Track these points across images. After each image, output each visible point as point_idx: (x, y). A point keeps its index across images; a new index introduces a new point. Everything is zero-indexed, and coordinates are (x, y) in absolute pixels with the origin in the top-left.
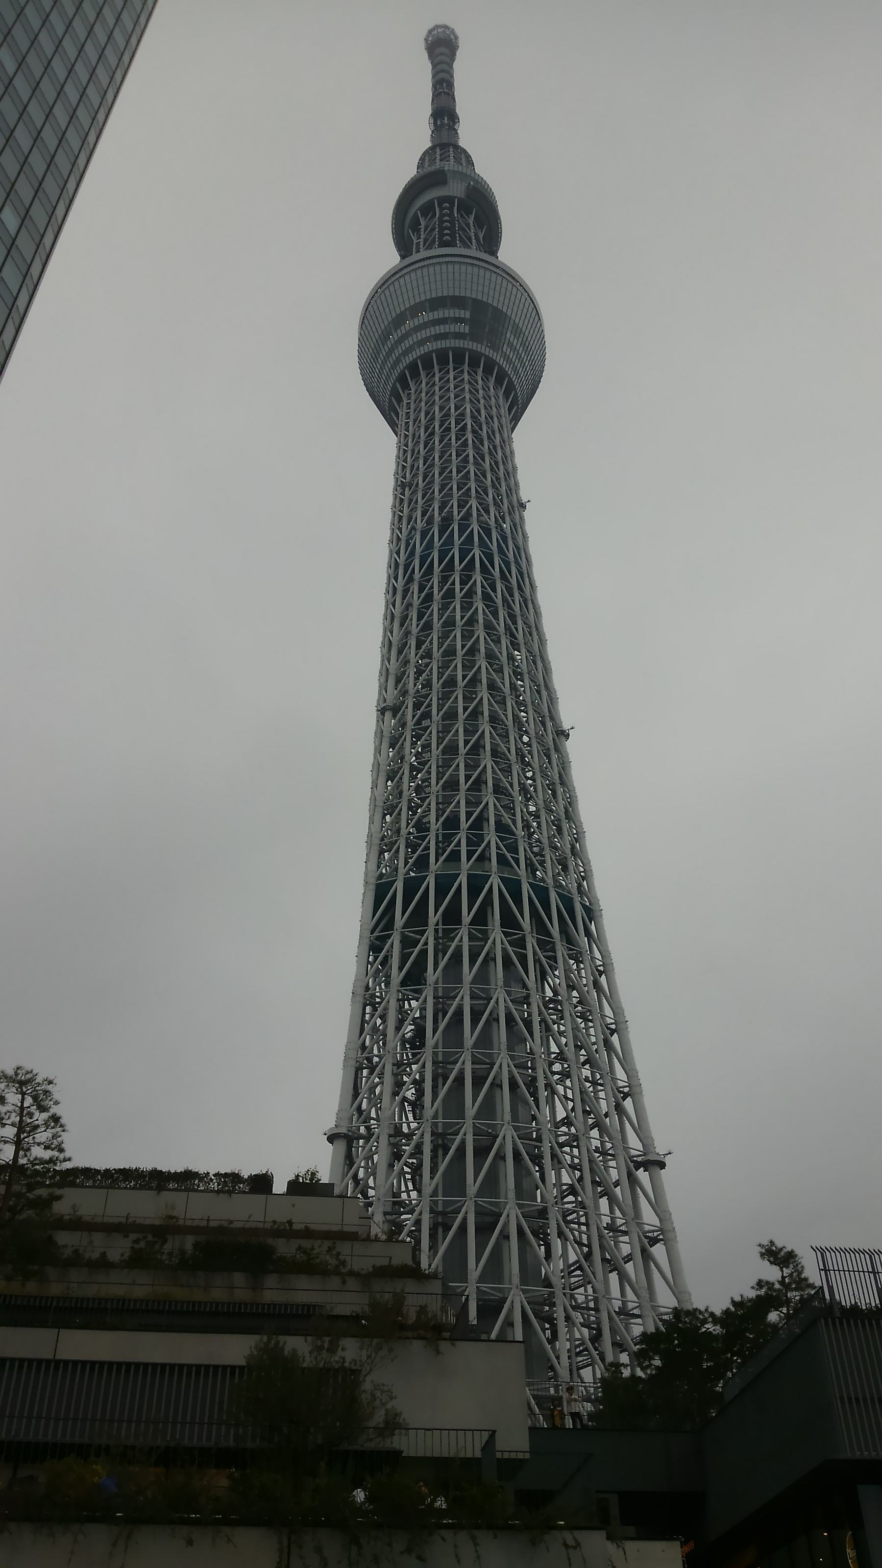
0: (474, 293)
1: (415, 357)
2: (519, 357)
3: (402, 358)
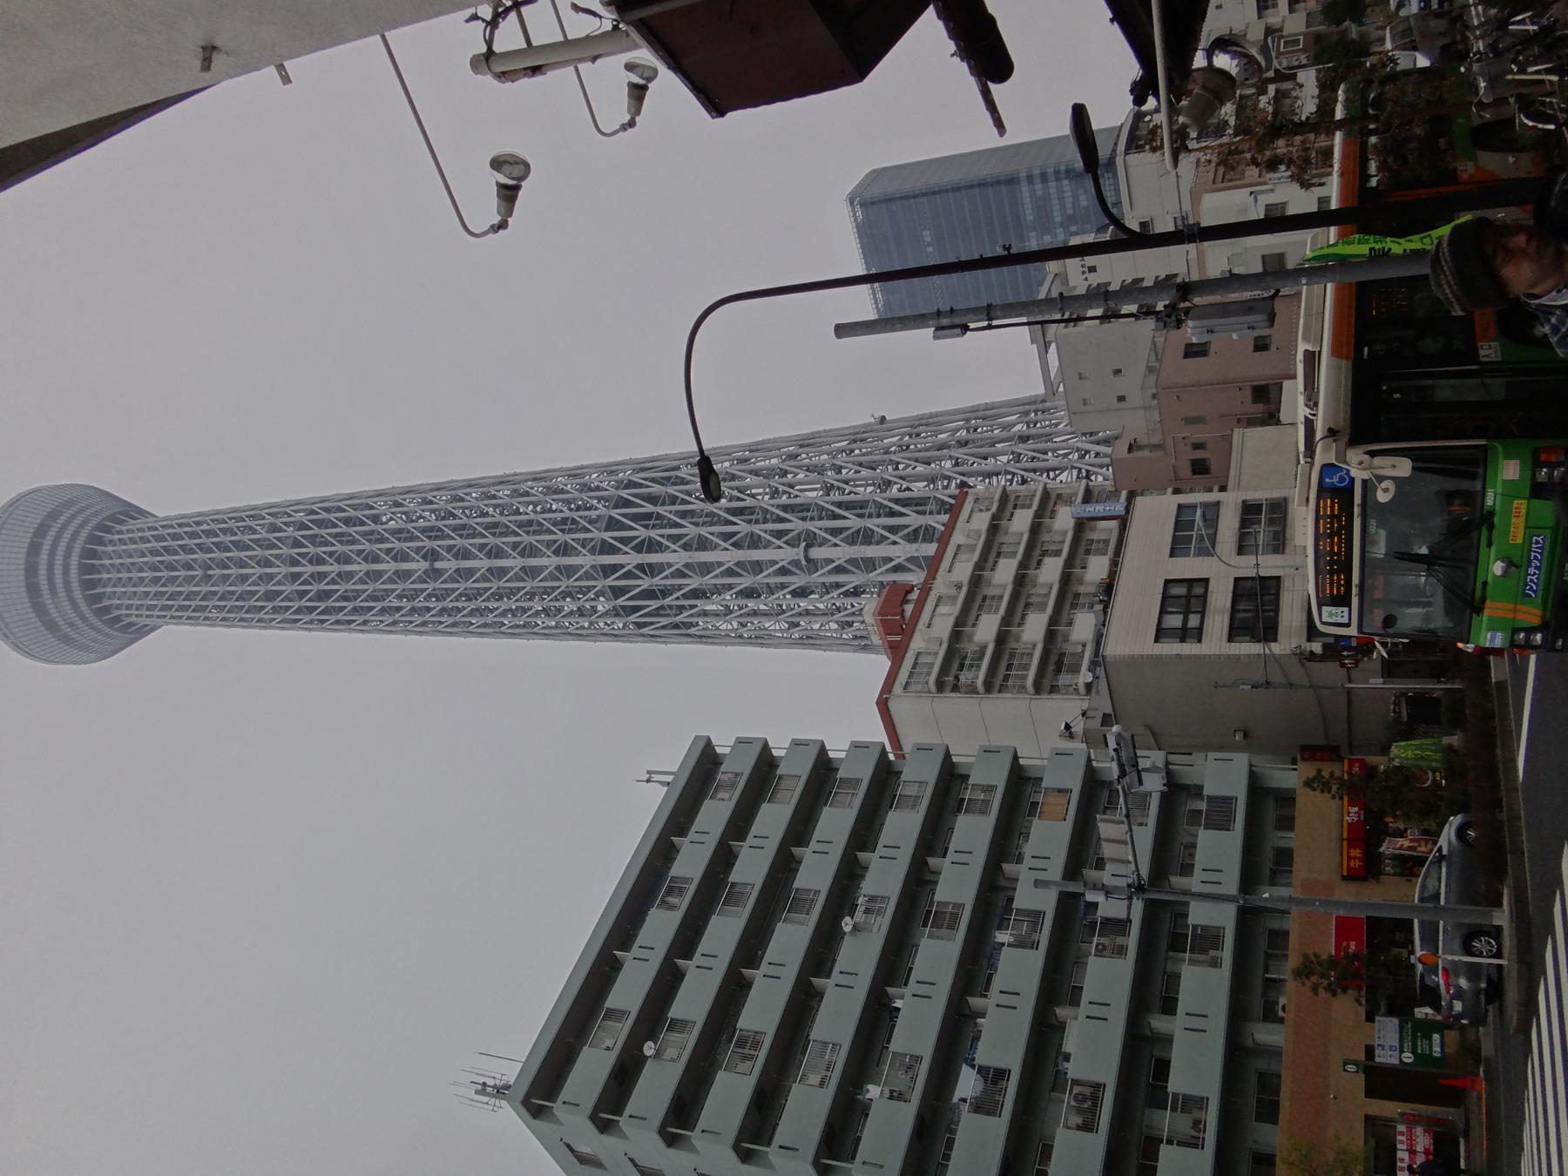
0: (21, 556)
1: (89, 611)
2: (79, 512)
3: (89, 623)
